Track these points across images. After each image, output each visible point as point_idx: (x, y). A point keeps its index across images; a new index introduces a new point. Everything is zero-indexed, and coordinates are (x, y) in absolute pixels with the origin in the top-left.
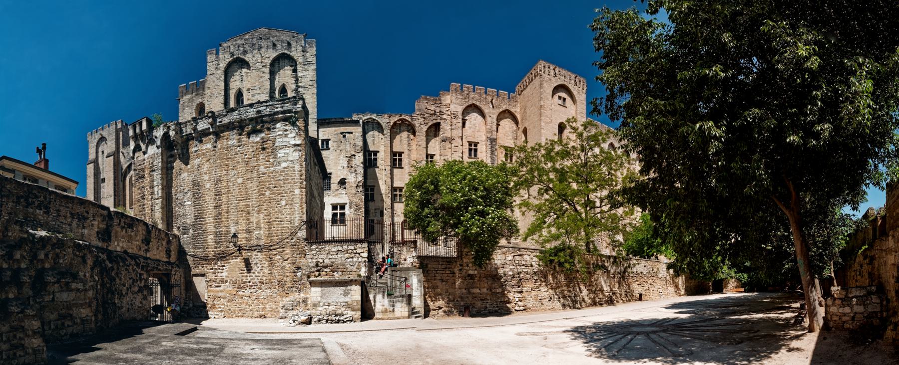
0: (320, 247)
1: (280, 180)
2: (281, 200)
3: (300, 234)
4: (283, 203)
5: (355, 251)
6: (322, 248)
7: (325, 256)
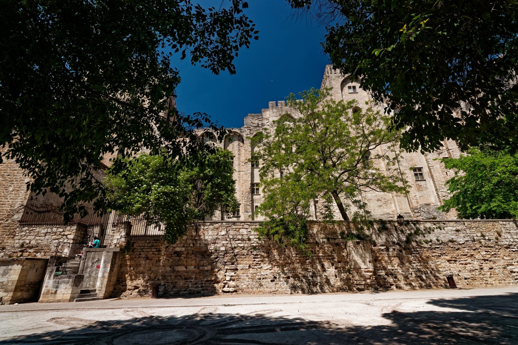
0: (31, 229)
1: (15, 170)
2: (10, 186)
3: (15, 217)
4: (11, 189)
5: (62, 233)
6: (33, 230)
7: (33, 237)
